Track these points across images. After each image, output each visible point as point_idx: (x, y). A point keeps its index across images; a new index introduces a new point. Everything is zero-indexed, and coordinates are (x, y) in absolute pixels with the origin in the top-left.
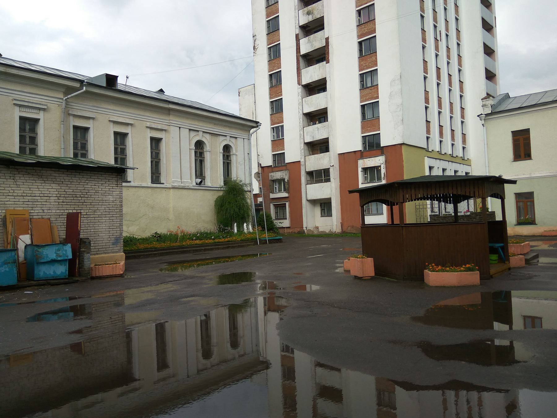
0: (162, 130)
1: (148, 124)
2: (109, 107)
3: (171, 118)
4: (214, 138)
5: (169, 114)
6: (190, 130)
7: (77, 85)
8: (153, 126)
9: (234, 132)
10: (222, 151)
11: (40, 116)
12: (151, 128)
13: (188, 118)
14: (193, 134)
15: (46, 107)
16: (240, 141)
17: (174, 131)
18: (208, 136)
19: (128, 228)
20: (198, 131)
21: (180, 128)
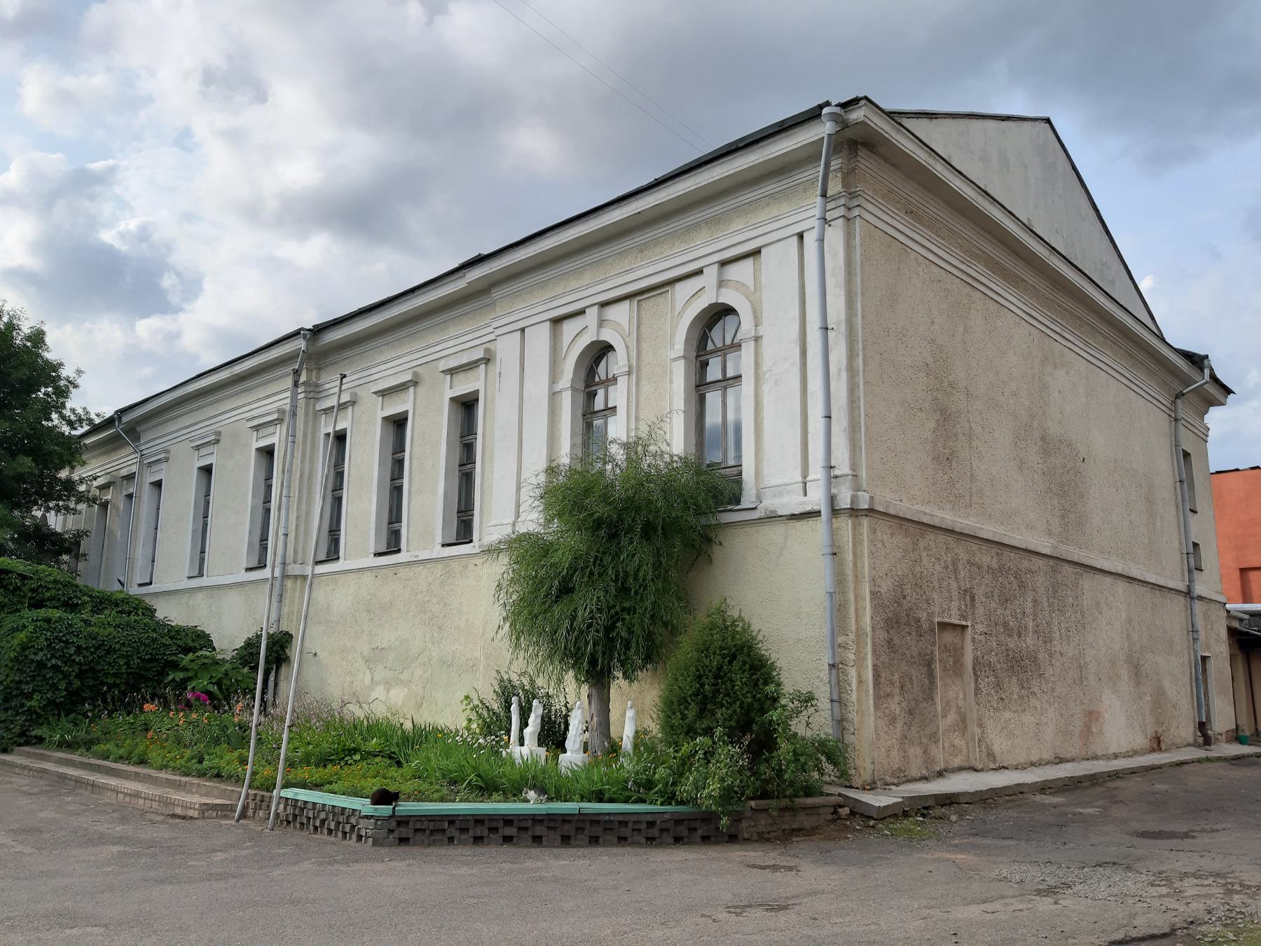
0: (471, 366)
1: (443, 365)
2: (383, 359)
3: (499, 311)
4: (652, 305)
5: (494, 303)
6: (557, 321)
7: (300, 344)
8: (453, 363)
9: (735, 237)
10: (679, 347)
11: (274, 440)
12: (452, 372)
13: (542, 285)
14: (570, 328)
15: (275, 416)
16: (779, 264)
17: (506, 349)
18: (620, 314)
19: (388, 691)
20: (581, 312)
21: (523, 330)
